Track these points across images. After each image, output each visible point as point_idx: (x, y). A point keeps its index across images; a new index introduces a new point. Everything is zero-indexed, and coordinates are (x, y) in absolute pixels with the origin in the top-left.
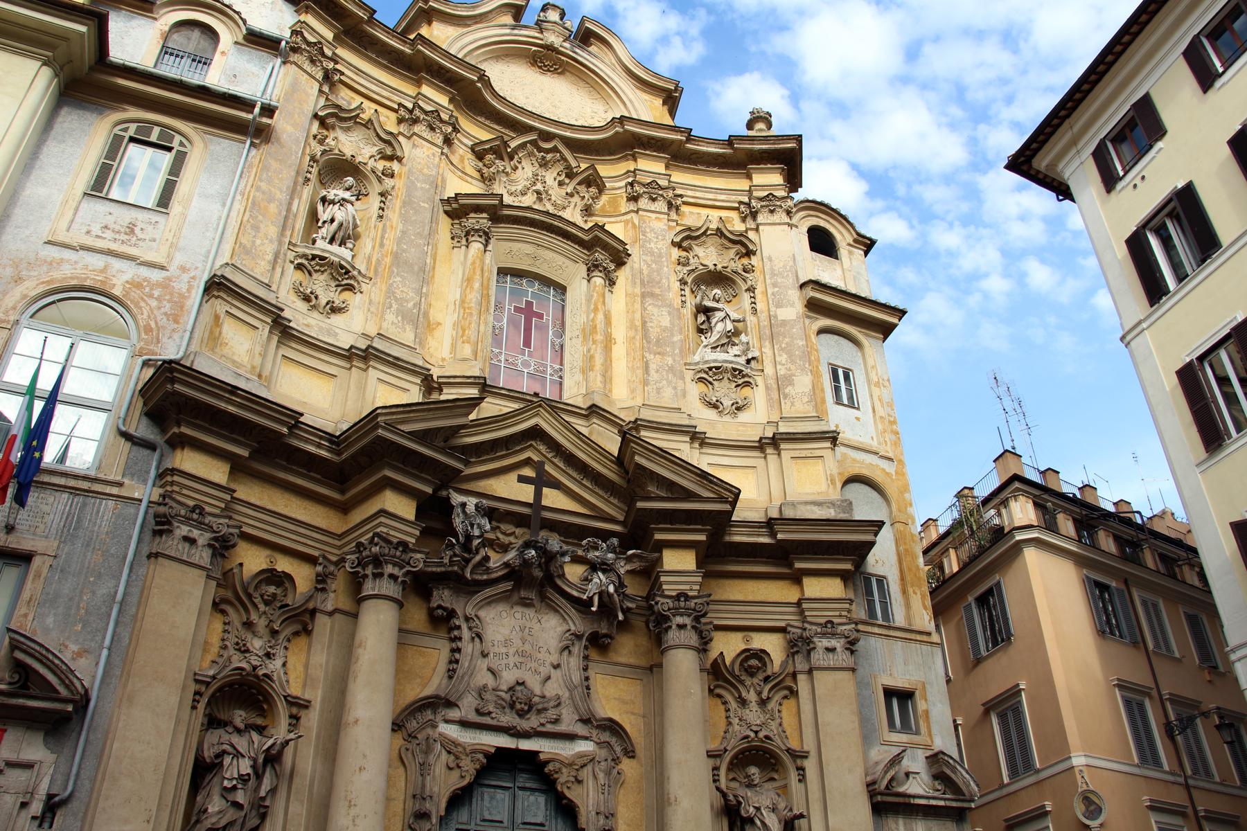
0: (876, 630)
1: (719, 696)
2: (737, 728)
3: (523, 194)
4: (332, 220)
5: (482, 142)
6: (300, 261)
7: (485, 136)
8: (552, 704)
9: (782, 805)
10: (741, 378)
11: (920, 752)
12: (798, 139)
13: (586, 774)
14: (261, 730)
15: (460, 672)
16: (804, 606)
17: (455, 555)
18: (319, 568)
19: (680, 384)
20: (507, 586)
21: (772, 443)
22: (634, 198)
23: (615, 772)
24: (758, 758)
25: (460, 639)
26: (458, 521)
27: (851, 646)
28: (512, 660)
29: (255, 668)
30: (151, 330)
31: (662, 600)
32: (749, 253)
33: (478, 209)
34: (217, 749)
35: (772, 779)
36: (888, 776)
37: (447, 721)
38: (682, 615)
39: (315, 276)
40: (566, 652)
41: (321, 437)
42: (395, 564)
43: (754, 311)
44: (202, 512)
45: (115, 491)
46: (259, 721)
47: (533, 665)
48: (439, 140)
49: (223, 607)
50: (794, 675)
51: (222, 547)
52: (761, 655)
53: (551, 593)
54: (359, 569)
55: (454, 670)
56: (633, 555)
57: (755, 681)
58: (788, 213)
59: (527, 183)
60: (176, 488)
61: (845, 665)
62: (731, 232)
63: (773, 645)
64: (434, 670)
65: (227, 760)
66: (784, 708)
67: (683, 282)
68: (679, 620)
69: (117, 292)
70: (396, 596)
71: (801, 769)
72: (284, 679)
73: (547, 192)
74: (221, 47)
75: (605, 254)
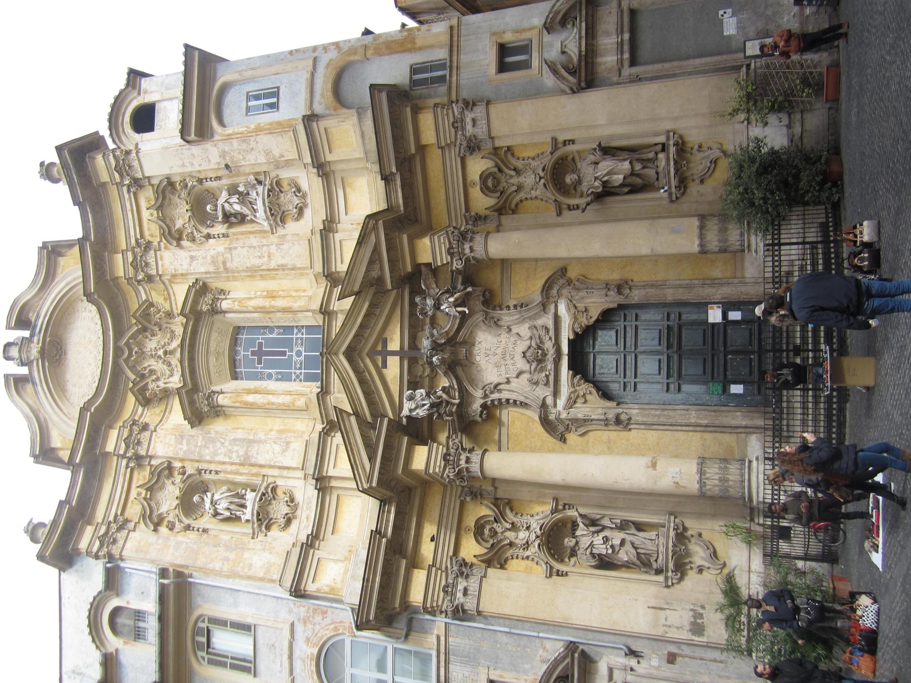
0: (454, 79)
1: (517, 205)
2: (538, 192)
3: (169, 365)
4: (228, 509)
5: (137, 399)
6: (263, 529)
7: (131, 399)
8: (535, 332)
9: (592, 158)
10: (275, 190)
11: (545, 39)
12: (59, 149)
13: (581, 306)
14: (575, 525)
15: (522, 399)
16: (443, 144)
17: (445, 412)
18: (468, 499)
19: (289, 237)
20: (459, 370)
21: (322, 169)
22: (150, 279)
23: (577, 283)
24: (560, 172)
25: (500, 400)
26: (421, 413)
27: (469, 105)
28: (509, 362)
29: (537, 537)
30: (335, 627)
31: (455, 262)
32: (171, 184)
33: (192, 403)
35: (573, 159)
36: (566, 75)
37: (555, 405)
38: (463, 249)
39: (272, 516)
40: (500, 323)
41: (384, 512)
42: (459, 460)
43: (218, 178)
44: (447, 586)
45: (443, 639)
46: (569, 525)
47: (511, 346)
48: (147, 434)
50: (496, 149)
52: (484, 177)
53: (460, 338)
55: (521, 403)
56: (425, 285)
57: (503, 179)
58: (128, 153)
59: (160, 362)
60: (435, 604)
61: (484, 111)
62: (157, 199)
63: (478, 166)
64: (522, 414)
65: (595, 551)
66: (521, 155)
67: (208, 237)
68: (467, 251)
69: (315, 651)
70: (481, 453)
71: (565, 143)
72: (541, 516)
73: (163, 347)
74: (123, 604)
75: (203, 303)
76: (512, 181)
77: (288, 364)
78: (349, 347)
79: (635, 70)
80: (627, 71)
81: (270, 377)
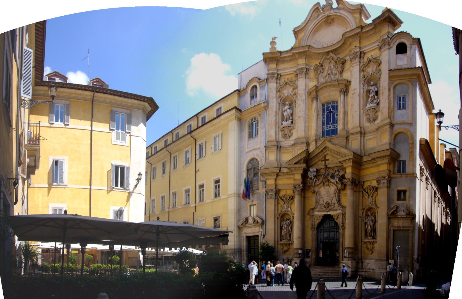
20: (322, 184)
77: (328, 124)
79: (392, 231)
80: (392, 229)
81: (324, 118)
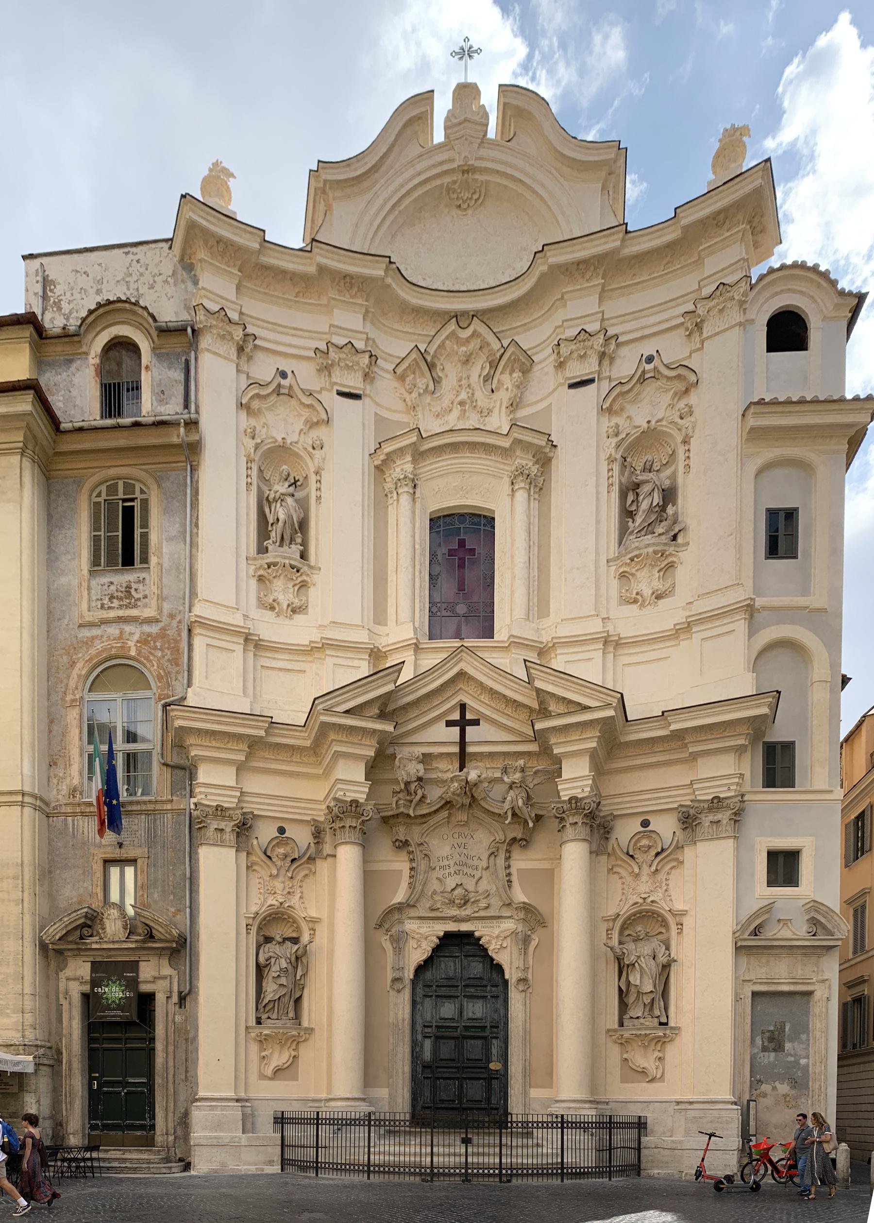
34: (267, 956)
49: (255, 867)
51: (244, 828)
54: (333, 825)
65: (273, 960)
76: (645, 868)
78: (471, 678)
